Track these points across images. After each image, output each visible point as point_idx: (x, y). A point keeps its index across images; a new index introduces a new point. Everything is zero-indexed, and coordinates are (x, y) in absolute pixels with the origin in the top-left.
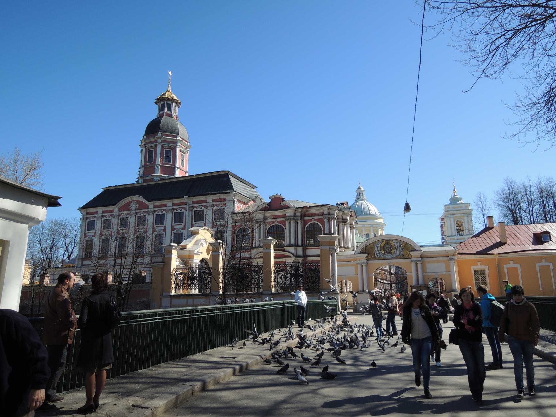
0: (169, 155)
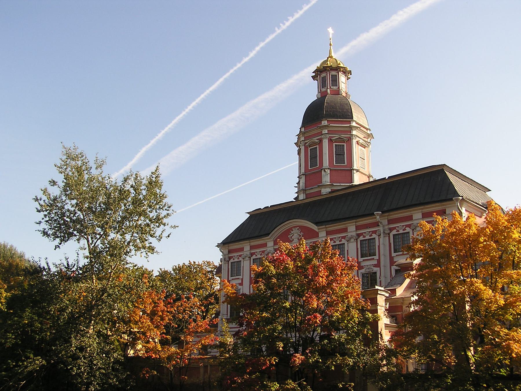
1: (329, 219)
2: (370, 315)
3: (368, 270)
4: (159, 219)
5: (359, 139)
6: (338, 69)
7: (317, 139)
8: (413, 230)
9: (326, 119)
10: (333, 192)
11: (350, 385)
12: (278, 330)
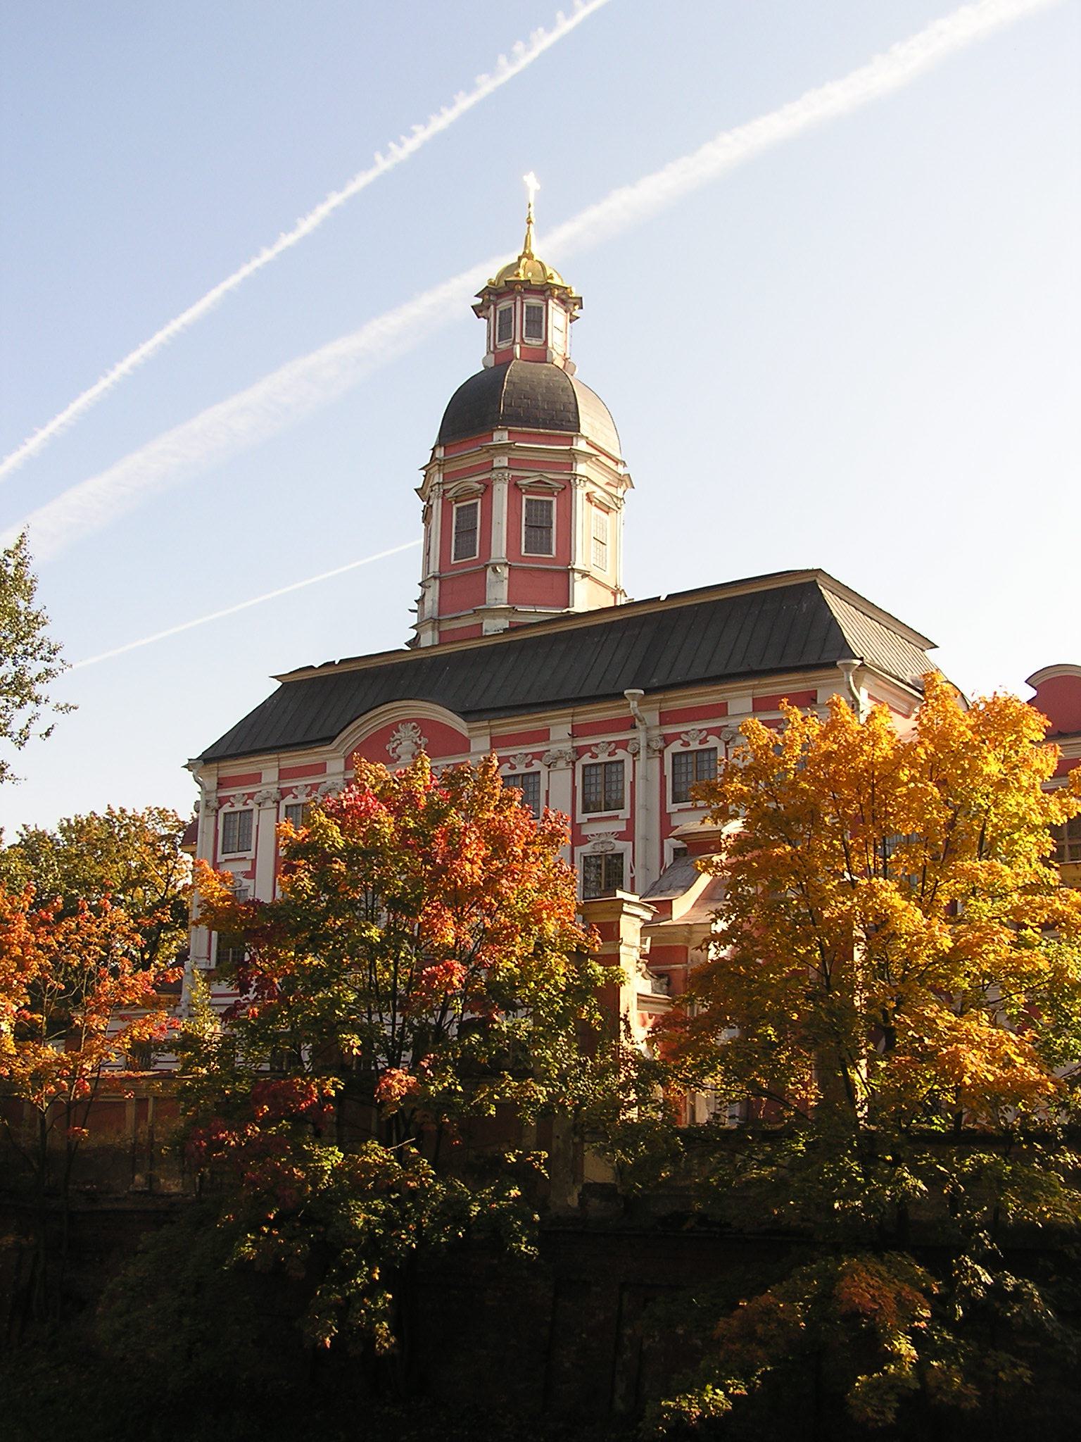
0: (546, 523)
1: (500, 705)
2: (599, 969)
3: (599, 848)
4: (22, 686)
5: (594, 488)
6: (545, 290)
8: (727, 743)
9: (507, 427)
10: (514, 628)
11: (538, 1157)
12: (347, 1004)
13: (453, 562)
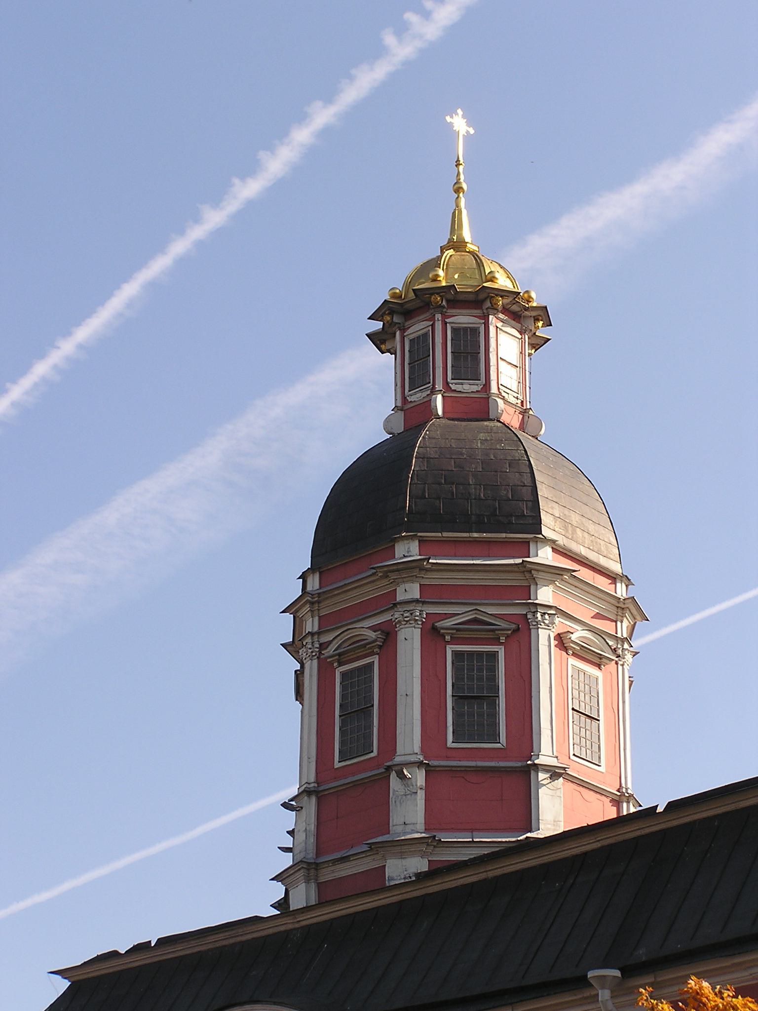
6: (483, 300)
7: (373, 628)
10: (435, 872)
13: (337, 765)
